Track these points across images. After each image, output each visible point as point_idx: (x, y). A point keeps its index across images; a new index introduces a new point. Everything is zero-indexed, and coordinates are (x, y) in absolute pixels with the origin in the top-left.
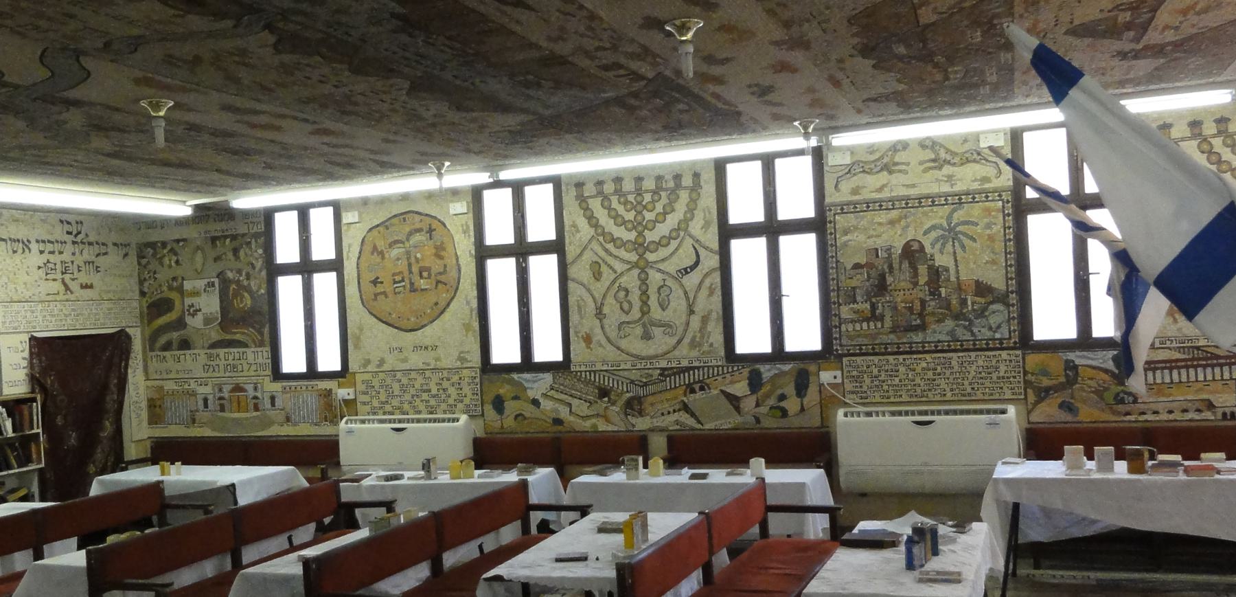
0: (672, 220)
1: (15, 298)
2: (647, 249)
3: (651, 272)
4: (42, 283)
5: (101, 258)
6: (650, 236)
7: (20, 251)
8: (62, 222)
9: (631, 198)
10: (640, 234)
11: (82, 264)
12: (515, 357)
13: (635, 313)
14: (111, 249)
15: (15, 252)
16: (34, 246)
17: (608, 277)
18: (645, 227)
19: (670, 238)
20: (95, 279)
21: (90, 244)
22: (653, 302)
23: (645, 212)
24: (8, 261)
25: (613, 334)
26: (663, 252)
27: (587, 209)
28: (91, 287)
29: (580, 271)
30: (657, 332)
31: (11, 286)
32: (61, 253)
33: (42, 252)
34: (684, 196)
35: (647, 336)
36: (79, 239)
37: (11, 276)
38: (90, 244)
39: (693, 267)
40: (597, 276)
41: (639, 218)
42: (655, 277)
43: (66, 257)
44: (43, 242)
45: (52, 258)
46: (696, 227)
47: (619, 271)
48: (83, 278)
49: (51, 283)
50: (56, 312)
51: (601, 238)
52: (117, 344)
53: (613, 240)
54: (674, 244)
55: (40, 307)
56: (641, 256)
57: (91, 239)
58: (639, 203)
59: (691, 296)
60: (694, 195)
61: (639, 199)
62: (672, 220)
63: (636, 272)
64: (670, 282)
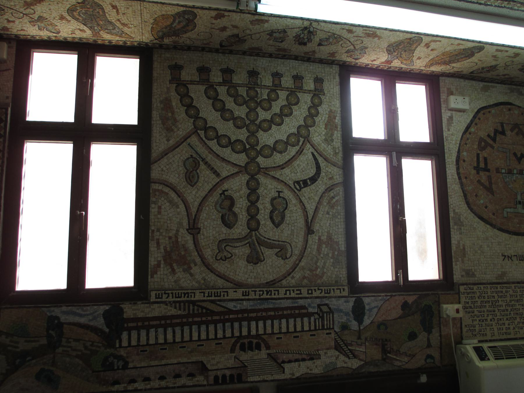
0: (290, 126)
2: (259, 153)
3: (262, 179)
6: (267, 138)
9: (242, 91)
10: (253, 134)
12: (58, 281)
13: (240, 229)
17: (206, 179)
18: (259, 127)
19: (287, 143)
22: (263, 217)
23: (259, 109)
25: (208, 253)
26: (278, 159)
27: (187, 95)
29: (170, 170)
30: (268, 252)
34: (306, 99)
35: (255, 259)
39: (314, 179)
40: (191, 178)
41: (252, 116)
42: (268, 188)
46: (318, 135)
47: (224, 174)
51: (202, 133)
53: (218, 137)
54: (292, 151)
56: (253, 160)
58: (252, 99)
59: (311, 213)
60: (316, 101)
61: (252, 93)
62: (290, 126)
63: (244, 178)
64: (287, 194)
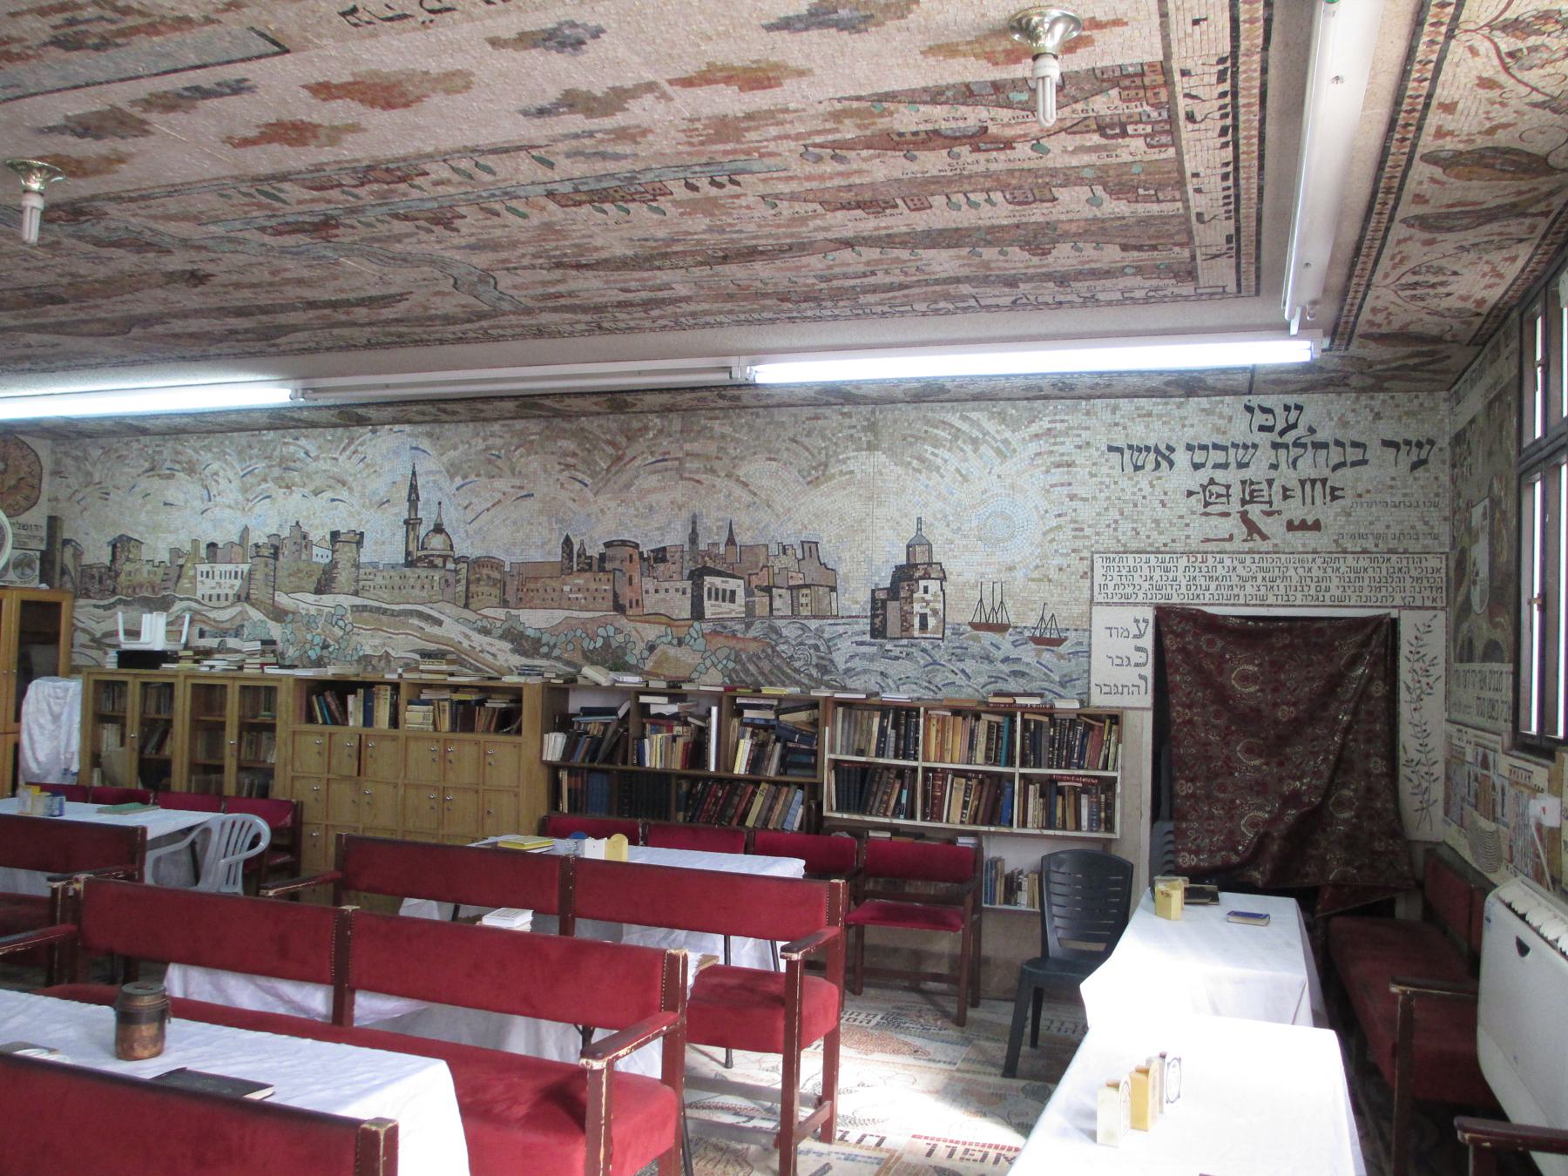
1: (1134, 545)
4: (1197, 521)
5: (1348, 472)
7: (1150, 466)
8: (1249, 409)
11: (1294, 484)
14: (1375, 451)
15: (1137, 468)
16: (1181, 458)
20: (1327, 512)
21: (1318, 446)
24: (1124, 483)
28: (1316, 526)
31: (1125, 526)
32: (1242, 465)
33: (1197, 466)
36: (1290, 437)
37: (1128, 509)
38: (1318, 446)
43: (1258, 470)
44: (1204, 447)
45: (1220, 475)
48: (1295, 510)
49: (1215, 521)
50: (1220, 571)
52: (1379, 637)
55: (1183, 562)
57: (1321, 436)
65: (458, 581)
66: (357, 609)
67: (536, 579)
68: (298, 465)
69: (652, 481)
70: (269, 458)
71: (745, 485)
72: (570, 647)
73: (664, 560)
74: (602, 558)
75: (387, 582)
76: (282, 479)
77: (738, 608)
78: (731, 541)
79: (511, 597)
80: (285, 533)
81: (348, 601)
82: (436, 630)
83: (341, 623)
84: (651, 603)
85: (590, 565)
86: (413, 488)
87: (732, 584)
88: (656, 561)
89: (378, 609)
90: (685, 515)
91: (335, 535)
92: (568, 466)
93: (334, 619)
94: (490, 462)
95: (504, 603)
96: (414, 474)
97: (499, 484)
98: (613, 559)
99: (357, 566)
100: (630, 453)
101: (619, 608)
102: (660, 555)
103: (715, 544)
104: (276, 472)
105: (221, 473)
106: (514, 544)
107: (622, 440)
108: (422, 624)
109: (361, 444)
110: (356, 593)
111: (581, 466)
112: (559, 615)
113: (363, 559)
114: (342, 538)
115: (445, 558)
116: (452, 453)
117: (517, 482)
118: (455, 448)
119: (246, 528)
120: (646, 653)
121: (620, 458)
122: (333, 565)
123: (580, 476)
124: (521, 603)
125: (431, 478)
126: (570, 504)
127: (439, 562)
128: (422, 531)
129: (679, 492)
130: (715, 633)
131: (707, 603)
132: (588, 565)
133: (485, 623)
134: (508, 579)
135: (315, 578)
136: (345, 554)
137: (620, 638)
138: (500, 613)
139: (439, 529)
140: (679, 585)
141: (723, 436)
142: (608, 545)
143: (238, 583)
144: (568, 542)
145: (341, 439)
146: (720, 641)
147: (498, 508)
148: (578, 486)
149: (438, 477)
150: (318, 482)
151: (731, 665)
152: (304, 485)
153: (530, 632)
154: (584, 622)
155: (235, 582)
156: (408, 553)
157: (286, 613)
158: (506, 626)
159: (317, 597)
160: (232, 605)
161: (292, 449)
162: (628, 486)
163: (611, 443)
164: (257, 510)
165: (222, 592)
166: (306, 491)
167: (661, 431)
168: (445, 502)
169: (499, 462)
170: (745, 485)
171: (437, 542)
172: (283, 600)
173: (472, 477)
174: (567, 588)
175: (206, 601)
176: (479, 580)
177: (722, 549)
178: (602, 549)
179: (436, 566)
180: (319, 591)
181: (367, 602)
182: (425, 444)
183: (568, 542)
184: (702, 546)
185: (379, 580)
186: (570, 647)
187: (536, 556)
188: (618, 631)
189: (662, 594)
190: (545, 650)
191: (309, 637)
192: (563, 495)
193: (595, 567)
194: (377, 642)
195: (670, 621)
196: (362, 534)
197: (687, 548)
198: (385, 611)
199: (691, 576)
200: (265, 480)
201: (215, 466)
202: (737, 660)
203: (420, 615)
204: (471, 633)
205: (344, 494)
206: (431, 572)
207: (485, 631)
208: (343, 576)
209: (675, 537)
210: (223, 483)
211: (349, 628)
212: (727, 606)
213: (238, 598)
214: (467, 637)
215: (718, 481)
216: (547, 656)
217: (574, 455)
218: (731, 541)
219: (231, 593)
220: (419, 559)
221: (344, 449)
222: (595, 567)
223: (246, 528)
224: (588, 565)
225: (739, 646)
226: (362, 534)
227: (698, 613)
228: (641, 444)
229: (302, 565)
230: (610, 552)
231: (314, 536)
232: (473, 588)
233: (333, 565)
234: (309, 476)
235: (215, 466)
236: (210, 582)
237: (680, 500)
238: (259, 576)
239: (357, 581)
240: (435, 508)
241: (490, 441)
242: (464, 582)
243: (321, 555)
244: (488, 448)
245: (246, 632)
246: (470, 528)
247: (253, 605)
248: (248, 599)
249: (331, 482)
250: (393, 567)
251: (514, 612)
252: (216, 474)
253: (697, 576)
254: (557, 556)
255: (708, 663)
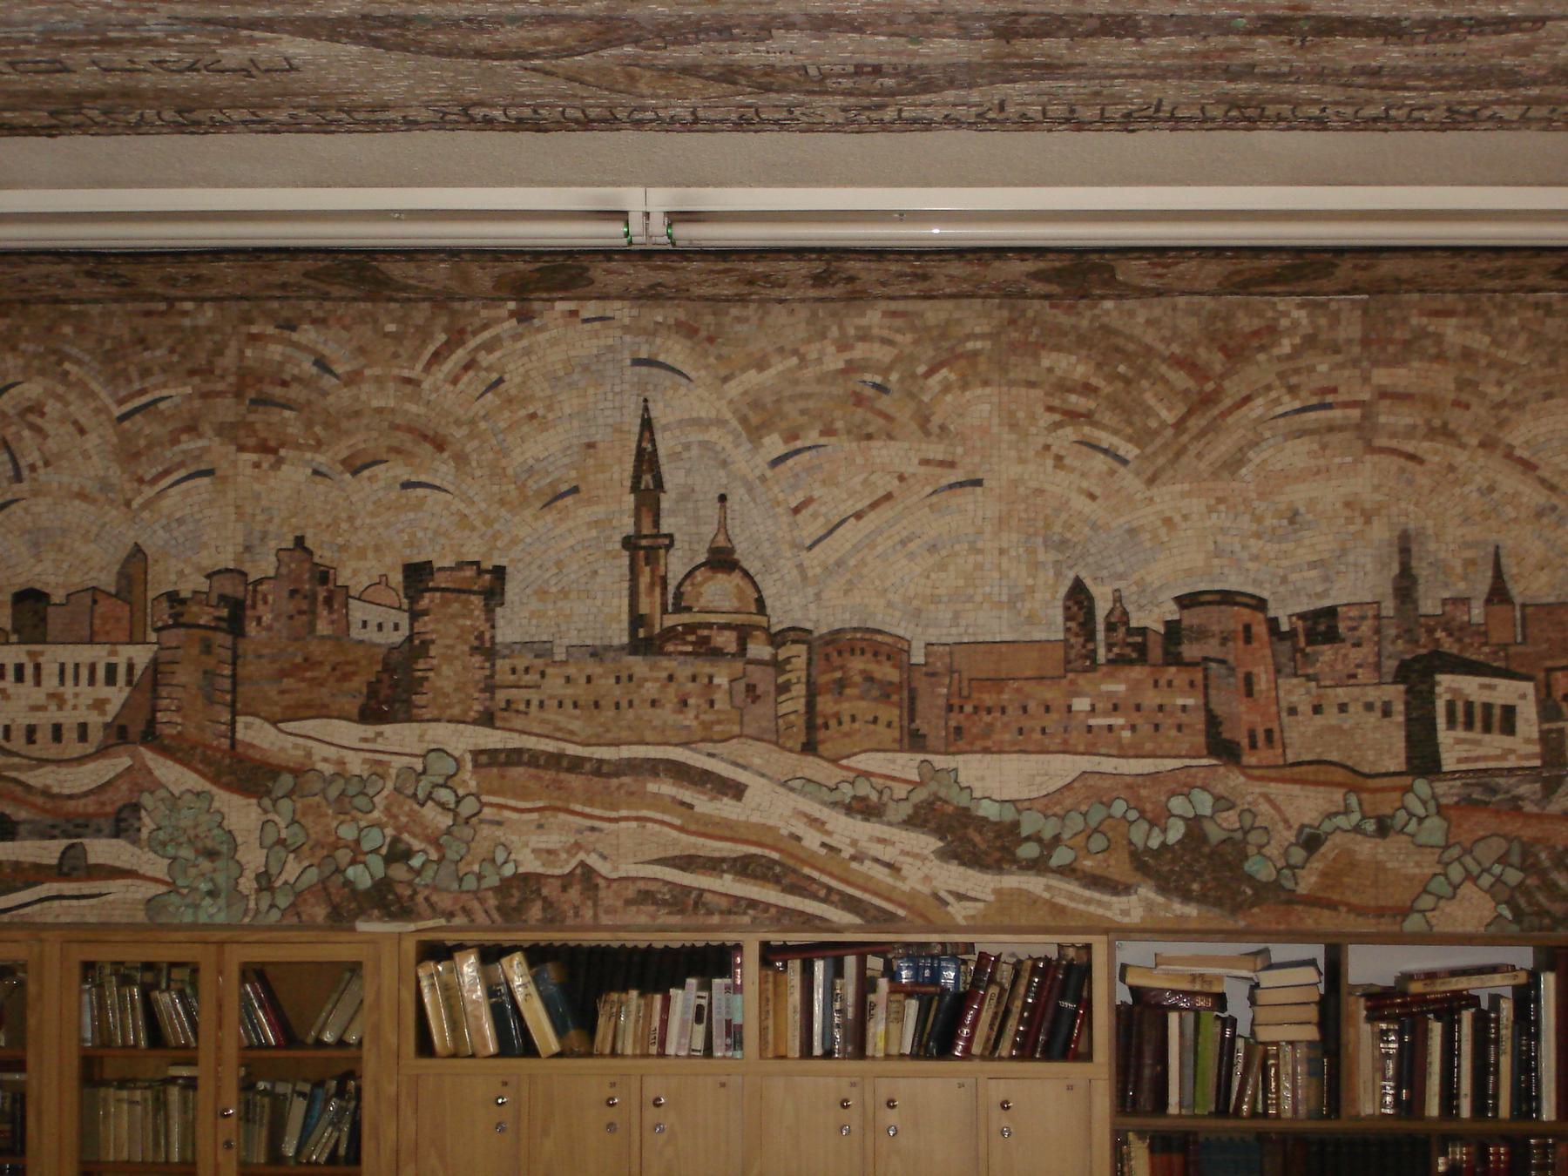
65: (784, 688)
66: (486, 759)
67: (998, 682)
68: (295, 392)
69: (1298, 453)
70: (206, 372)
71: (1528, 466)
72: (1098, 842)
73: (1332, 637)
74: (1173, 631)
75: (580, 690)
76: (249, 426)
77: (1522, 746)
78: (1499, 593)
79: (931, 721)
80: (264, 565)
81: (464, 739)
82: (727, 808)
83: (445, 795)
84: (1302, 736)
85: (1142, 649)
86: (647, 461)
87: (1505, 691)
88: (1312, 638)
89: (555, 761)
90: (1380, 532)
91: (417, 575)
92: (1073, 416)
93: (416, 786)
94: (859, 400)
95: (914, 741)
96: (647, 425)
97: (882, 452)
98: (1201, 634)
99: (487, 650)
100: (1234, 388)
101: (1223, 748)
102: (1322, 625)
103: (1463, 601)
104: (227, 410)
105: (52, 408)
106: (935, 600)
107: (1217, 361)
108: (687, 795)
109: (489, 347)
110: (487, 719)
111: (1107, 418)
112: (1064, 768)
113: (506, 633)
114: (441, 580)
115: (744, 633)
116: (752, 377)
117: (937, 451)
118: (762, 365)
119: (138, 550)
120: (1298, 855)
121: (1207, 400)
122: (416, 648)
123: (1105, 439)
124: (958, 740)
125: (695, 436)
126: (1079, 503)
127: (727, 641)
128: (676, 565)
129: (1364, 479)
130: (1469, 804)
131: (1445, 736)
132: (1135, 649)
133: (863, 789)
134: (921, 684)
135: (358, 683)
136: (448, 627)
137: (1230, 819)
138: (905, 765)
139: (722, 560)
140: (1373, 694)
141: (1468, 355)
142: (1186, 602)
143: (117, 696)
144: (1079, 596)
145: (425, 334)
146: (1481, 823)
147: (886, 512)
148: (1100, 462)
149: (713, 434)
150: (360, 440)
151: (1513, 876)
152: (319, 445)
153: (988, 810)
154: (1132, 785)
155: (103, 691)
156: (637, 620)
157: (274, 771)
158: (921, 795)
159: (370, 730)
160: (102, 752)
161: (275, 351)
162: (1233, 464)
163: (1186, 364)
164: (166, 504)
165: (69, 718)
166: (321, 459)
167: (1311, 341)
168: (737, 496)
169: (884, 402)
170: (1528, 466)
171: (719, 593)
172: (258, 735)
173: (812, 437)
174: (1081, 704)
175: (18, 742)
176: (841, 685)
177: (1477, 613)
178: (1171, 612)
179: (717, 653)
180: (371, 714)
181: (531, 743)
182: (675, 351)
183: (1079, 596)
184: (1429, 605)
185: (554, 685)
186: (1098, 842)
187: (996, 627)
188: (1223, 803)
189: (1331, 717)
190: (1029, 851)
191: (348, 832)
192: (1059, 484)
193: (1156, 653)
194: (552, 840)
195: (1356, 779)
196: (499, 572)
197: (1389, 607)
198: (576, 765)
199: (1404, 673)
200: (192, 429)
201: (33, 389)
202: (1528, 864)
203: (680, 772)
204: (824, 813)
205: (442, 470)
206: (705, 668)
207: (865, 809)
208: (448, 673)
209: (1360, 584)
210: (59, 436)
211: (469, 806)
212: (1495, 743)
213: (119, 734)
214: (815, 823)
215: (1461, 457)
216: (1037, 866)
217: (1087, 389)
218: (1499, 593)
219: (94, 719)
220: (670, 634)
221: (437, 357)
222: (1156, 653)
223: (138, 550)
224: (1135, 649)
225: (1528, 833)
226: (499, 572)
227: (1423, 758)
228: (1261, 369)
229: (315, 649)
230: (1193, 618)
231: (354, 574)
232: (825, 704)
233: (416, 648)
234: (332, 423)
235: (33, 389)
236: (28, 693)
237: (1369, 498)
238: (185, 676)
239: (490, 688)
240: (711, 511)
241: (859, 351)
242: (799, 690)
243: (377, 624)
244: (850, 368)
245: (148, 823)
246: (813, 560)
247: (166, 751)
248: (150, 736)
249: (406, 440)
250: (596, 653)
251: (940, 761)
252: (37, 409)
253: (1417, 675)
254: (1052, 625)
255: (1456, 872)
